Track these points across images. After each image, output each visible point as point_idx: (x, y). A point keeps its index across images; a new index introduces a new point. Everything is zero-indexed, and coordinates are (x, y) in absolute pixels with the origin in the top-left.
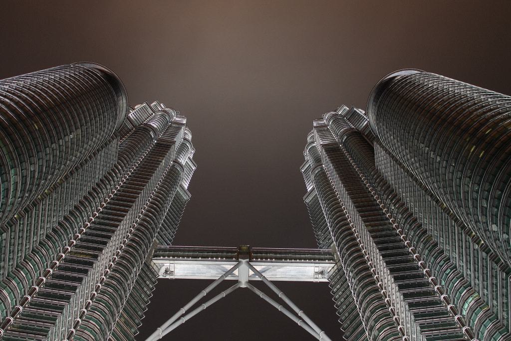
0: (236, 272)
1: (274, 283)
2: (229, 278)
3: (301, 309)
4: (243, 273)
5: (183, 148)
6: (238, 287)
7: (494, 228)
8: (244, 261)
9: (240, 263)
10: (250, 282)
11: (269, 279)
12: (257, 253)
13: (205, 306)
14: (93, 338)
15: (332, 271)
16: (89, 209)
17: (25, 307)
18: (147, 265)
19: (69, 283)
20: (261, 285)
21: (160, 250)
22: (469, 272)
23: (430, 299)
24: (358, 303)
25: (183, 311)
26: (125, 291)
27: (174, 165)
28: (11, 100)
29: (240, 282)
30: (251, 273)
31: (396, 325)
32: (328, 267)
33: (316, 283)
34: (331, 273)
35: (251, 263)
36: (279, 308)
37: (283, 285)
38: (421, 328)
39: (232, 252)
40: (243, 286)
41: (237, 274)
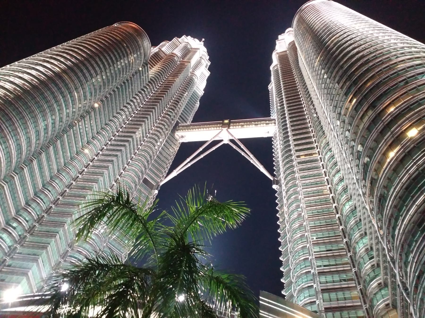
1: (241, 140)
2: (217, 139)
3: (252, 153)
5: (198, 64)
8: (225, 129)
9: (222, 130)
13: (202, 156)
25: (188, 160)
27: (191, 75)
35: (228, 130)
36: (243, 154)
39: (220, 124)
40: (226, 141)
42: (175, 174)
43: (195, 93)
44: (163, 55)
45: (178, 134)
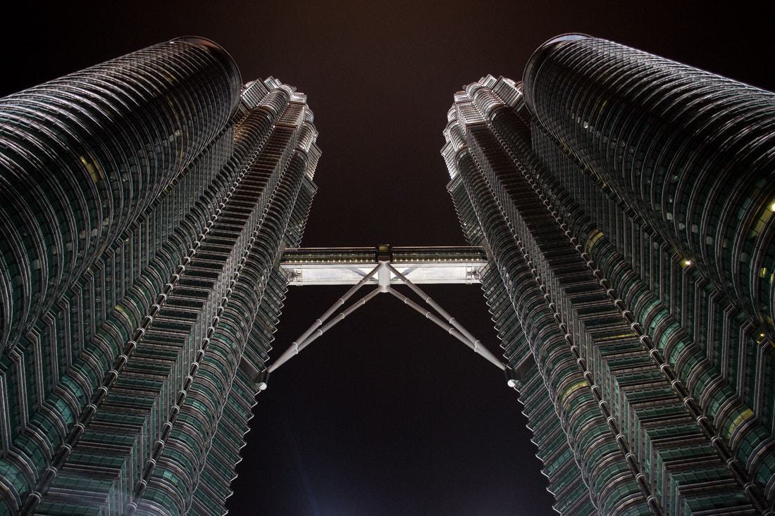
0: (376, 276)
2: (369, 282)
3: (452, 316)
4: (385, 277)
5: (304, 133)
6: (378, 292)
7: (669, 216)
8: (384, 263)
9: (380, 265)
10: (392, 286)
11: (413, 283)
12: (398, 252)
13: (343, 316)
14: (220, 371)
15: (485, 271)
16: (188, 238)
17: (147, 329)
18: (275, 272)
19: (193, 299)
20: (404, 289)
21: (287, 253)
22: (638, 264)
23: (595, 293)
24: (518, 308)
25: (320, 322)
26: (254, 303)
27: (296, 153)
28: (112, 91)
29: (380, 286)
30: (393, 275)
31: (562, 333)
32: (479, 265)
33: (469, 285)
34: (483, 273)
36: (427, 315)
37: (428, 288)
38: (593, 337)
39: (369, 252)
41: (377, 278)
42: (295, 350)
43: (304, 190)
44: (243, 110)
45: (287, 267)
